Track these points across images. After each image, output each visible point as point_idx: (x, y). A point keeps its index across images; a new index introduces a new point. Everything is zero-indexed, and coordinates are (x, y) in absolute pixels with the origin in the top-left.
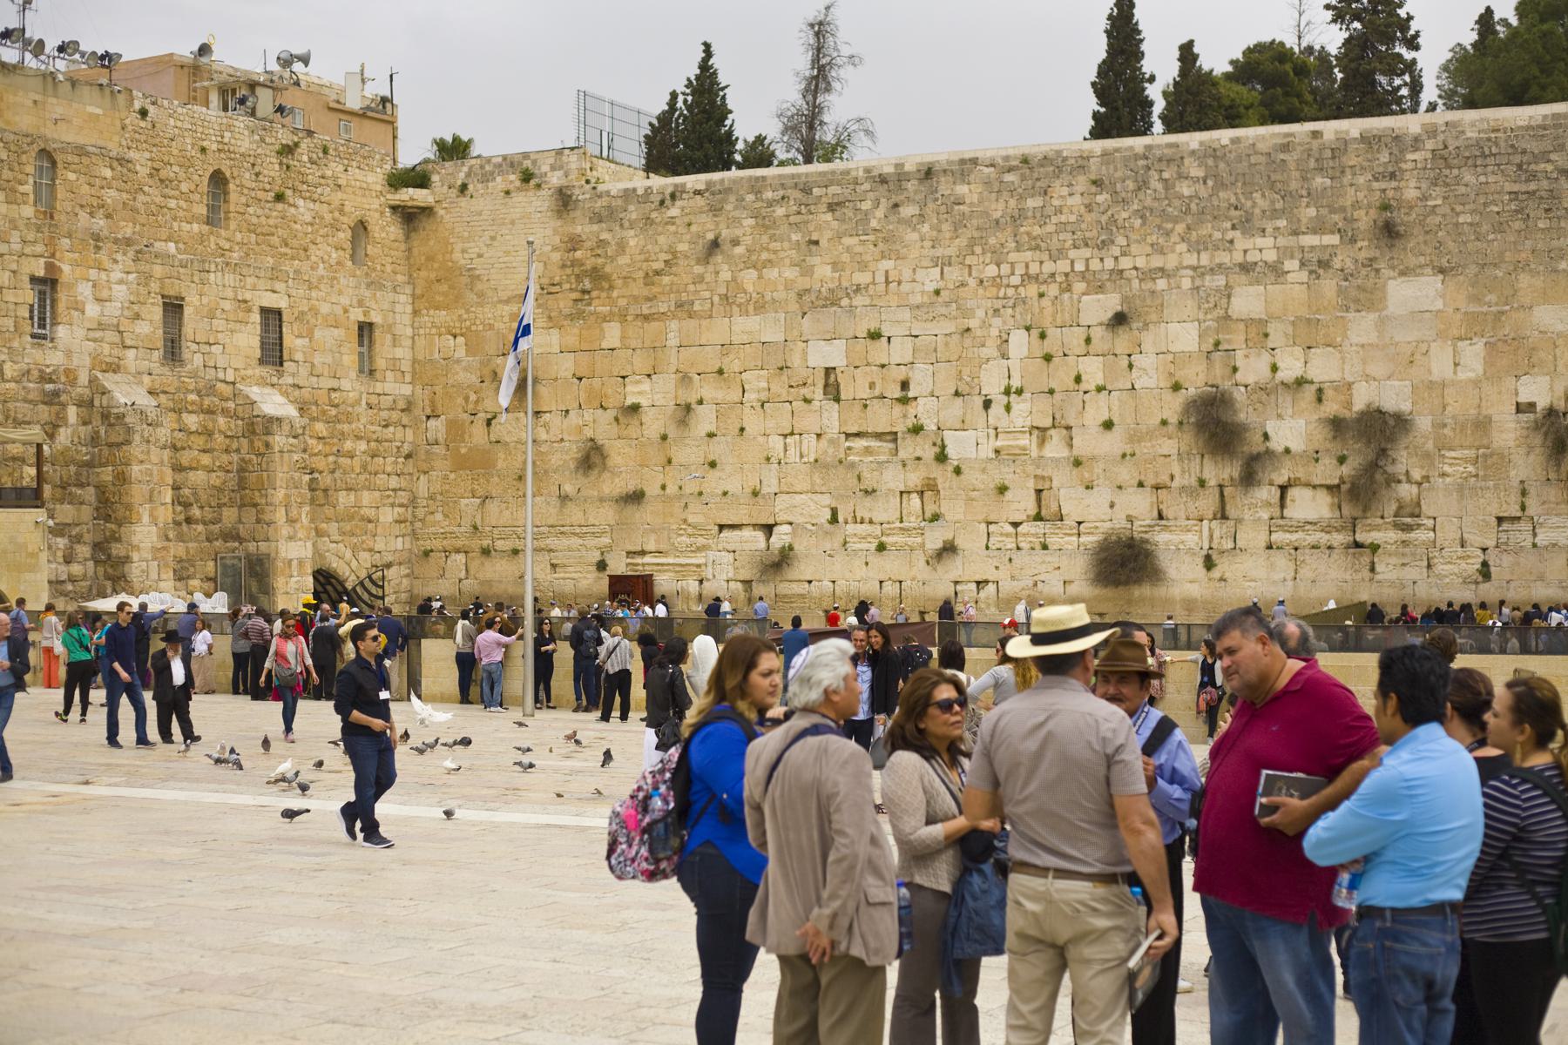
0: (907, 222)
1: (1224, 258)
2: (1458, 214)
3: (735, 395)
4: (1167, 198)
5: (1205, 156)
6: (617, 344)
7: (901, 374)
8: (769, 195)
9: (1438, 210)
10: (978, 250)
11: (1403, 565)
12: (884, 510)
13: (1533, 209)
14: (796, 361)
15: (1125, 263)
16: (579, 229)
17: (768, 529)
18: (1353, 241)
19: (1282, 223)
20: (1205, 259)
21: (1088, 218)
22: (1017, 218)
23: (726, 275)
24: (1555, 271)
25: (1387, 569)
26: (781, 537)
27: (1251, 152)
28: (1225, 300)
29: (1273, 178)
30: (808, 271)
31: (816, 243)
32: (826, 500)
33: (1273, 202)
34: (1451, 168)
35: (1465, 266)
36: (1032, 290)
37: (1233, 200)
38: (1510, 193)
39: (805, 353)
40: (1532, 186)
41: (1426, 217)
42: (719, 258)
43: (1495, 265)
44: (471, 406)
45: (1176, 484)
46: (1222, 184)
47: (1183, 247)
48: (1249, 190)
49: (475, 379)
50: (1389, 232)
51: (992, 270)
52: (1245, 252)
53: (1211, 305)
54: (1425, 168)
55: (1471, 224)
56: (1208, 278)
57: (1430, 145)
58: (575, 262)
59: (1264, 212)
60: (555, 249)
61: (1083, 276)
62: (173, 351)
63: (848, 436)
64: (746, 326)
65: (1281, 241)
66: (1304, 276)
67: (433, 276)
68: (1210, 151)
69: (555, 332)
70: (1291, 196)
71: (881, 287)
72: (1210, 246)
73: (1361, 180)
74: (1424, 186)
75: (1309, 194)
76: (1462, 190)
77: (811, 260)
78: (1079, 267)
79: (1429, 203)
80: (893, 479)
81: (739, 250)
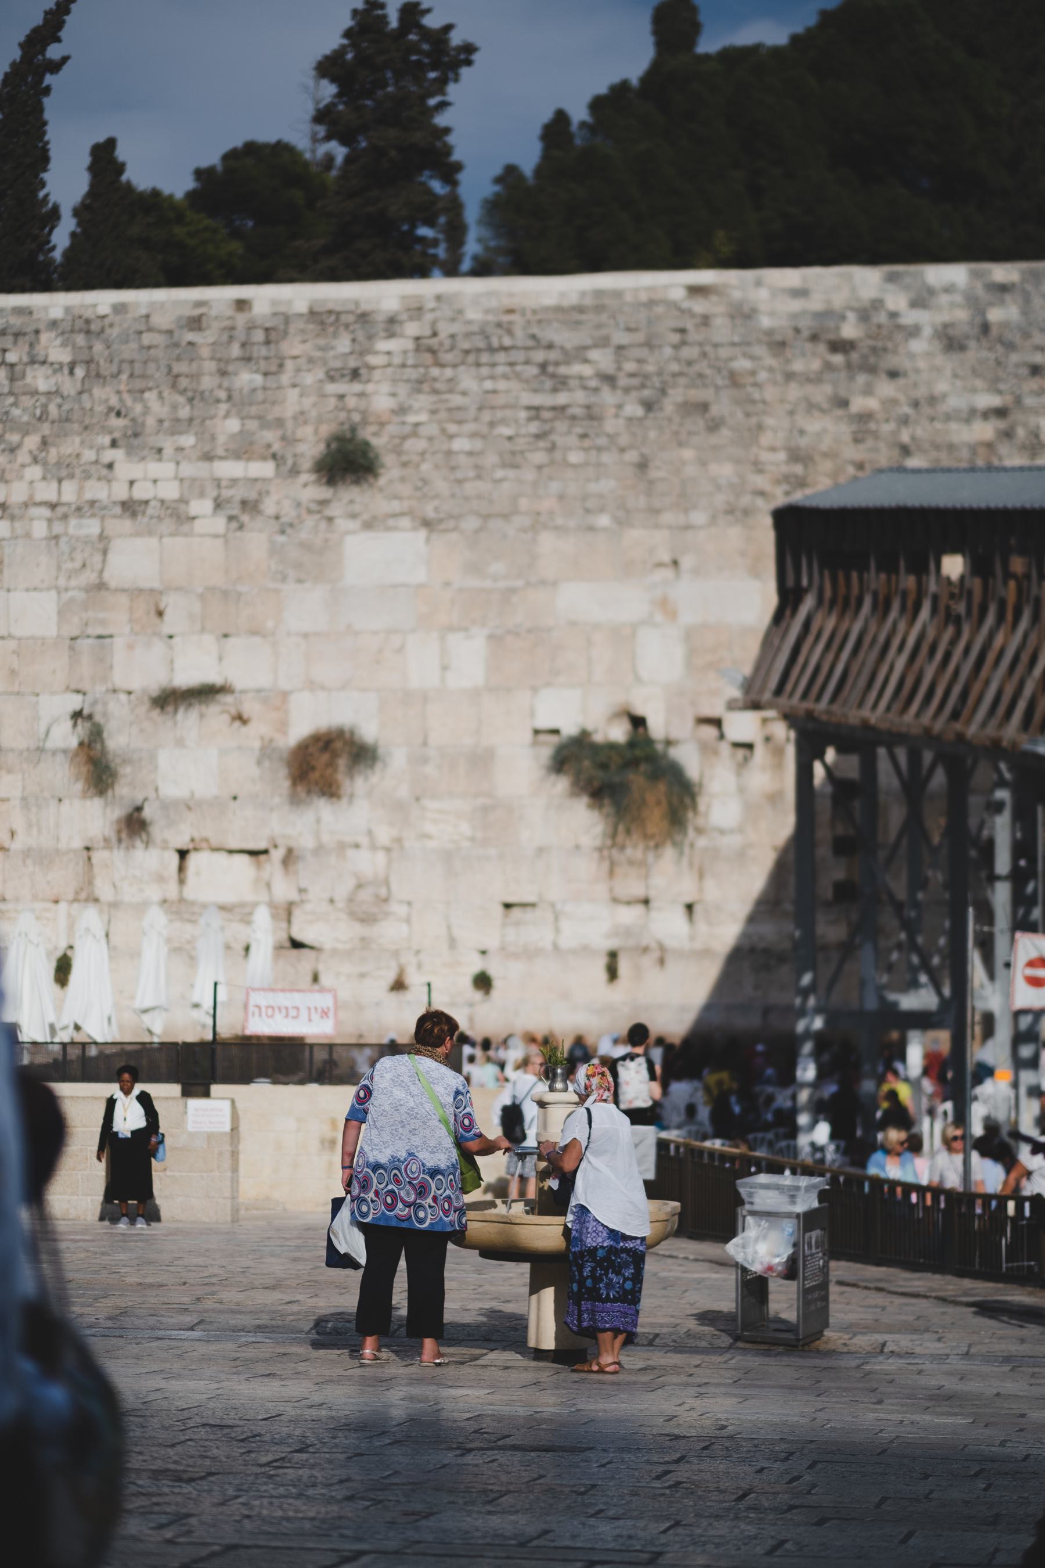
1: (97, 491)
2: (451, 437)
4: (11, 393)
5: (72, 331)
9: (423, 431)
11: (362, 976)
13: (564, 435)
18: (295, 472)
19: (188, 440)
20: (69, 492)
24: (591, 529)
27: (143, 327)
28: (98, 558)
29: (180, 368)
33: (175, 407)
34: (442, 366)
35: (458, 517)
37: (114, 401)
38: (529, 408)
40: (562, 398)
41: (404, 438)
43: (506, 517)
45: (17, 845)
46: (98, 375)
47: (35, 472)
48: (139, 384)
52: (132, 483)
53: (78, 564)
54: (404, 365)
55: (470, 454)
56: (73, 522)
57: (412, 329)
59: (161, 421)
65: (188, 469)
66: (220, 524)
68: (79, 324)
70: (203, 399)
72: (78, 472)
73: (309, 379)
74: (403, 390)
75: (230, 398)
76: (457, 400)
79: (412, 419)
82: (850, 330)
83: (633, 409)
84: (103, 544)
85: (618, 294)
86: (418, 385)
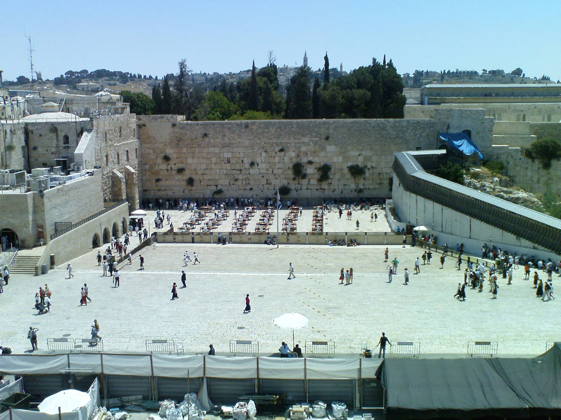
0: (243, 132)
3: (209, 162)
6: (185, 152)
7: (242, 159)
8: (216, 126)
12: (239, 183)
14: (222, 156)
15: (283, 141)
16: (176, 130)
17: (217, 186)
19: (309, 136)
20: (296, 141)
21: (276, 133)
25: (326, 192)
26: (219, 187)
30: (223, 140)
32: (228, 181)
36: (266, 145)
39: (223, 155)
42: (205, 138)
44: (154, 163)
47: (292, 139)
49: (155, 157)
50: (327, 138)
51: (258, 141)
57: (334, 124)
58: (176, 137)
60: (172, 134)
61: (275, 143)
62: (119, 163)
64: (211, 150)
69: (172, 149)
71: (238, 144)
73: (323, 129)
78: (274, 142)
81: (210, 136)
82: (381, 126)
83: (358, 133)
84: (300, 147)
86: (335, 131)
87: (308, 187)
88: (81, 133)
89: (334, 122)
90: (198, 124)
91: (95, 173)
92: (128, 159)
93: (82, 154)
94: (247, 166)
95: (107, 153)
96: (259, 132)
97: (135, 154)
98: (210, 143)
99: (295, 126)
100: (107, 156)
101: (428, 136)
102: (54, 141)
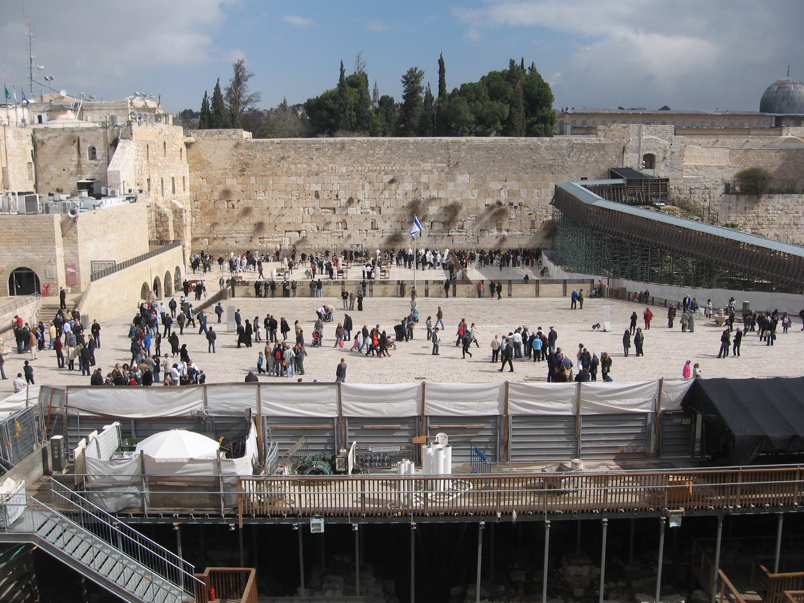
10: (356, 163)
12: (332, 227)
15: (394, 168)
17: (299, 232)
19: (432, 160)
22: (368, 155)
23: (286, 165)
26: (303, 234)
31: (312, 159)
36: (371, 173)
42: (283, 161)
44: (208, 198)
47: (408, 165)
49: (210, 191)
51: (360, 168)
63: (322, 208)
65: (432, 165)
66: (437, 173)
67: (195, 162)
77: (311, 163)
78: (383, 168)
80: (334, 219)
82: (532, 147)
83: (500, 158)
85: (498, 140)
86: (468, 153)
87: (431, 234)
88: (115, 143)
89: (468, 141)
90: (272, 143)
91: (139, 199)
92: (174, 192)
93: (119, 172)
94: (344, 202)
95: (150, 176)
96: (361, 154)
97: (182, 185)
98: (291, 169)
99: (412, 147)
100: (148, 180)
101: (597, 161)
102: (73, 156)
